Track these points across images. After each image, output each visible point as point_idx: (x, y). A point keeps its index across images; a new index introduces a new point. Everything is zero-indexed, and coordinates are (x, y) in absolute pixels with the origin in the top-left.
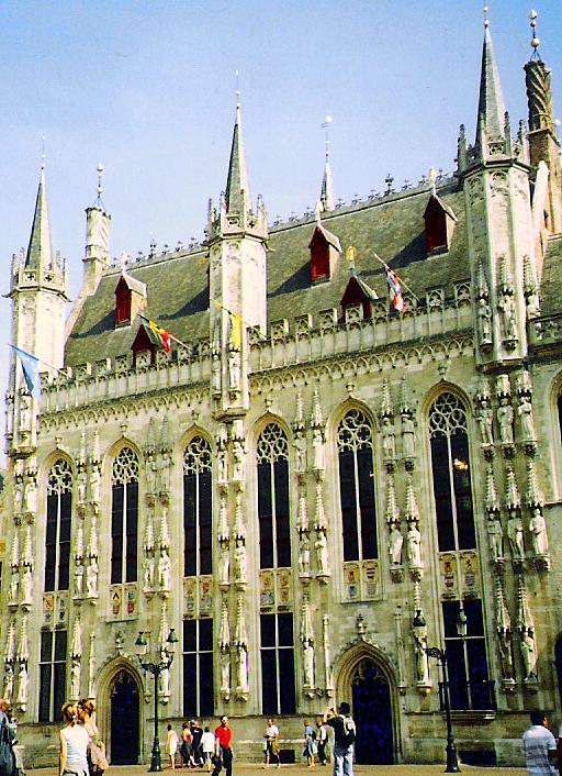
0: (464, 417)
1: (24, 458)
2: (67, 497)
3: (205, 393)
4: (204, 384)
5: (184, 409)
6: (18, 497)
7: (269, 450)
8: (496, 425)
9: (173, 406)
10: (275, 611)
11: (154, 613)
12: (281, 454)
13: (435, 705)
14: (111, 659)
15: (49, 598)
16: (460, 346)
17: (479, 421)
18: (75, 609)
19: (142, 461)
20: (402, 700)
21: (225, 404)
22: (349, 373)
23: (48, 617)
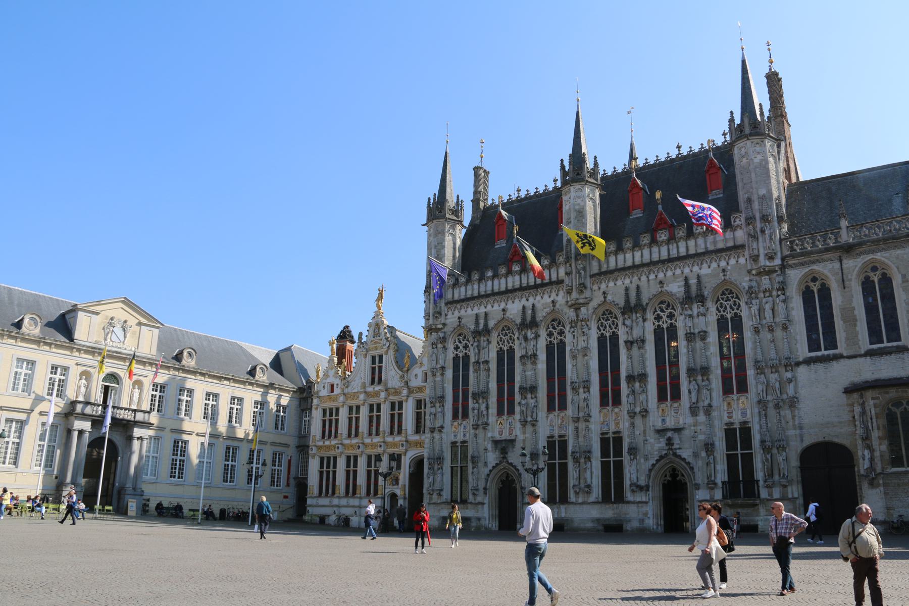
0: (739, 306)
2: (466, 357)
3: (561, 288)
4: (560, 282)
5: (547, 299)
6: (434, 357)
7: (606, 327)
8: (761, 310)
9: (538, 298)
10: (611, 435)
11: (528, 435)
12: (614, 330)
13: (718, 494)
14: (497, 464)
15: (456, 423)
16: (736, 256)
17: (750, 307)
18: (473, 431)
19: (517, 335)
20: (697, 491)
21: (575, 295)
23: (455, 436)
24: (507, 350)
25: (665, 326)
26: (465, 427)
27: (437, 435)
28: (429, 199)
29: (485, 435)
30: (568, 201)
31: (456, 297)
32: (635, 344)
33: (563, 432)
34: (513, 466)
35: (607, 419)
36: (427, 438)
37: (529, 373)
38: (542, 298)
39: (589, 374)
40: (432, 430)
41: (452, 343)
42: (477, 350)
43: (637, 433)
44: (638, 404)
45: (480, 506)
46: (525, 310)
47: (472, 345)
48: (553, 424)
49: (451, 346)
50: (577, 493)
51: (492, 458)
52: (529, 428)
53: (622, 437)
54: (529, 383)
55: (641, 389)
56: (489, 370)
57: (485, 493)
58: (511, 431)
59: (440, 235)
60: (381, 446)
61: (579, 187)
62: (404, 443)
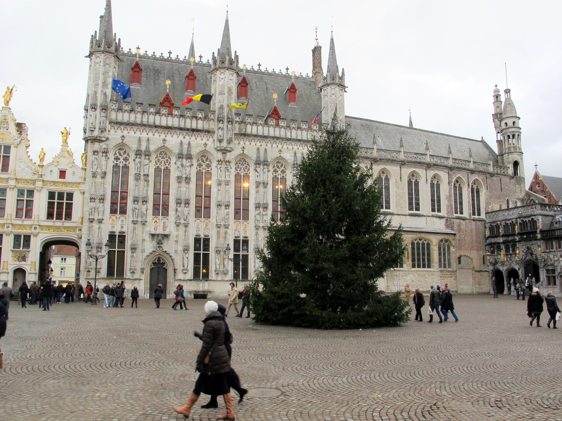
1: (99, 142)
2: (126, 167)
3: (211, 136)
7: (241, 169)
9: (193, 138)
10: (241, 238)
11: (179, 233)
14: (154, 252)
15: (114, 218)
18: (132, 225)
19: (173, 160)
22: (280, 146)
23: (113, 227)
24: (164, 169)
25: (279, 177)
26: (122, 221)
27: (95, 225)
28: (96, 32)
29: (143, 229)
30: (222, 79)
31: (120, 119)
32: (261, 184)
33: (207, 234)
34: (168, 254)
35: (239, 228)
36: (85, 226)
37: (183, 189)
38: (196, 139)
39: (229, 198)
40: (91, 221)
41: (113, 154)
42: (139, 165)
43: (260, 239)
44: (261, 221)
45: (137, 281)
46: (183, 144)
47: (134, 160)
48: (200, 227)
49: (111, 156)
50: (217, 274)
51: (149, 246)
52: (182, 228)
53: (248, 240)
54: (183, 197)
55: (264, 213)
56: (149, 181)
57: (143, 272)
58: (164, 228)
59: (107, 66)
60: (9, 227)
61: (232, 72)
62: (38, 227)
